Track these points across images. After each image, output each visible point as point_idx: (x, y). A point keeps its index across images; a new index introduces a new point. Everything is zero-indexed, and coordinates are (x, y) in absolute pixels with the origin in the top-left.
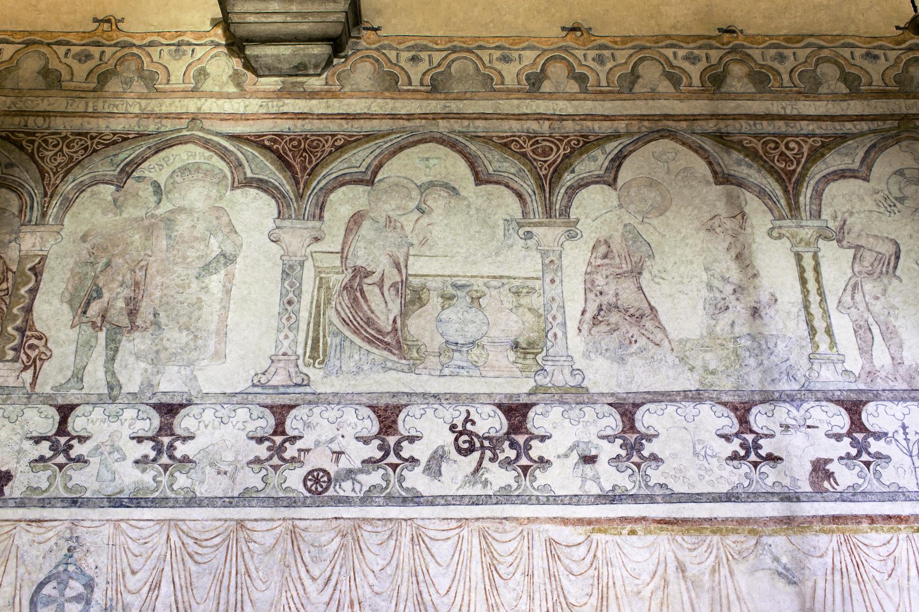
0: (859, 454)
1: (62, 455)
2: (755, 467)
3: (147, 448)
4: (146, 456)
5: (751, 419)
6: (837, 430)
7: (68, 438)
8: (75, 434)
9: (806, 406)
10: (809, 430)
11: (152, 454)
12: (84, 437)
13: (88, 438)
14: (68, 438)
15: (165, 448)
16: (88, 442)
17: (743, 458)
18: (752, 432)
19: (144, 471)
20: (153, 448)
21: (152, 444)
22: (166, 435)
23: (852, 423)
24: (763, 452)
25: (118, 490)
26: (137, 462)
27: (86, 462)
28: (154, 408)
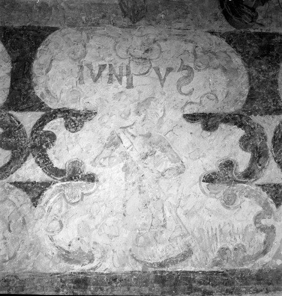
1: (31, 161)
3: (227, 143)
4: (229, 165)
7: (38, 115)
8: (54, 106)
11: (243, 159)
12: (77, 114)
13: (88, 115)
14: (38, 115)
15: (269, 144)
16: (87, 125)
19: (229, 202)
20: (245, 143)
21: (240, 132)
22: (268, 112)
25: (177, 249)
26: (210, 179)
27: (91, 178)
28: (229, 42)
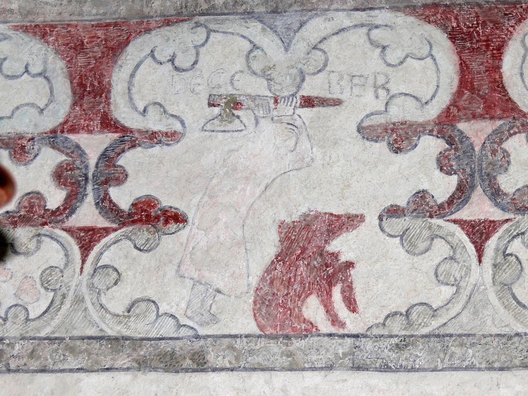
0: (462, 195)
2: (86, 249)
5: (118, 79)
6: (403, 111)
9: (316, 27)
10: (306, 113)
17: (55, 217)
18: (108, 123)
23: (466, 83)
24: (123, 197)
